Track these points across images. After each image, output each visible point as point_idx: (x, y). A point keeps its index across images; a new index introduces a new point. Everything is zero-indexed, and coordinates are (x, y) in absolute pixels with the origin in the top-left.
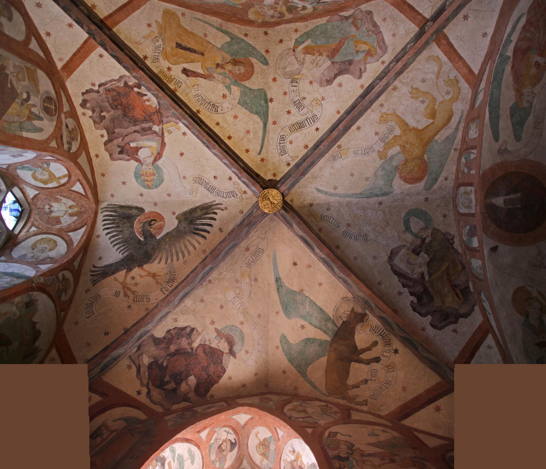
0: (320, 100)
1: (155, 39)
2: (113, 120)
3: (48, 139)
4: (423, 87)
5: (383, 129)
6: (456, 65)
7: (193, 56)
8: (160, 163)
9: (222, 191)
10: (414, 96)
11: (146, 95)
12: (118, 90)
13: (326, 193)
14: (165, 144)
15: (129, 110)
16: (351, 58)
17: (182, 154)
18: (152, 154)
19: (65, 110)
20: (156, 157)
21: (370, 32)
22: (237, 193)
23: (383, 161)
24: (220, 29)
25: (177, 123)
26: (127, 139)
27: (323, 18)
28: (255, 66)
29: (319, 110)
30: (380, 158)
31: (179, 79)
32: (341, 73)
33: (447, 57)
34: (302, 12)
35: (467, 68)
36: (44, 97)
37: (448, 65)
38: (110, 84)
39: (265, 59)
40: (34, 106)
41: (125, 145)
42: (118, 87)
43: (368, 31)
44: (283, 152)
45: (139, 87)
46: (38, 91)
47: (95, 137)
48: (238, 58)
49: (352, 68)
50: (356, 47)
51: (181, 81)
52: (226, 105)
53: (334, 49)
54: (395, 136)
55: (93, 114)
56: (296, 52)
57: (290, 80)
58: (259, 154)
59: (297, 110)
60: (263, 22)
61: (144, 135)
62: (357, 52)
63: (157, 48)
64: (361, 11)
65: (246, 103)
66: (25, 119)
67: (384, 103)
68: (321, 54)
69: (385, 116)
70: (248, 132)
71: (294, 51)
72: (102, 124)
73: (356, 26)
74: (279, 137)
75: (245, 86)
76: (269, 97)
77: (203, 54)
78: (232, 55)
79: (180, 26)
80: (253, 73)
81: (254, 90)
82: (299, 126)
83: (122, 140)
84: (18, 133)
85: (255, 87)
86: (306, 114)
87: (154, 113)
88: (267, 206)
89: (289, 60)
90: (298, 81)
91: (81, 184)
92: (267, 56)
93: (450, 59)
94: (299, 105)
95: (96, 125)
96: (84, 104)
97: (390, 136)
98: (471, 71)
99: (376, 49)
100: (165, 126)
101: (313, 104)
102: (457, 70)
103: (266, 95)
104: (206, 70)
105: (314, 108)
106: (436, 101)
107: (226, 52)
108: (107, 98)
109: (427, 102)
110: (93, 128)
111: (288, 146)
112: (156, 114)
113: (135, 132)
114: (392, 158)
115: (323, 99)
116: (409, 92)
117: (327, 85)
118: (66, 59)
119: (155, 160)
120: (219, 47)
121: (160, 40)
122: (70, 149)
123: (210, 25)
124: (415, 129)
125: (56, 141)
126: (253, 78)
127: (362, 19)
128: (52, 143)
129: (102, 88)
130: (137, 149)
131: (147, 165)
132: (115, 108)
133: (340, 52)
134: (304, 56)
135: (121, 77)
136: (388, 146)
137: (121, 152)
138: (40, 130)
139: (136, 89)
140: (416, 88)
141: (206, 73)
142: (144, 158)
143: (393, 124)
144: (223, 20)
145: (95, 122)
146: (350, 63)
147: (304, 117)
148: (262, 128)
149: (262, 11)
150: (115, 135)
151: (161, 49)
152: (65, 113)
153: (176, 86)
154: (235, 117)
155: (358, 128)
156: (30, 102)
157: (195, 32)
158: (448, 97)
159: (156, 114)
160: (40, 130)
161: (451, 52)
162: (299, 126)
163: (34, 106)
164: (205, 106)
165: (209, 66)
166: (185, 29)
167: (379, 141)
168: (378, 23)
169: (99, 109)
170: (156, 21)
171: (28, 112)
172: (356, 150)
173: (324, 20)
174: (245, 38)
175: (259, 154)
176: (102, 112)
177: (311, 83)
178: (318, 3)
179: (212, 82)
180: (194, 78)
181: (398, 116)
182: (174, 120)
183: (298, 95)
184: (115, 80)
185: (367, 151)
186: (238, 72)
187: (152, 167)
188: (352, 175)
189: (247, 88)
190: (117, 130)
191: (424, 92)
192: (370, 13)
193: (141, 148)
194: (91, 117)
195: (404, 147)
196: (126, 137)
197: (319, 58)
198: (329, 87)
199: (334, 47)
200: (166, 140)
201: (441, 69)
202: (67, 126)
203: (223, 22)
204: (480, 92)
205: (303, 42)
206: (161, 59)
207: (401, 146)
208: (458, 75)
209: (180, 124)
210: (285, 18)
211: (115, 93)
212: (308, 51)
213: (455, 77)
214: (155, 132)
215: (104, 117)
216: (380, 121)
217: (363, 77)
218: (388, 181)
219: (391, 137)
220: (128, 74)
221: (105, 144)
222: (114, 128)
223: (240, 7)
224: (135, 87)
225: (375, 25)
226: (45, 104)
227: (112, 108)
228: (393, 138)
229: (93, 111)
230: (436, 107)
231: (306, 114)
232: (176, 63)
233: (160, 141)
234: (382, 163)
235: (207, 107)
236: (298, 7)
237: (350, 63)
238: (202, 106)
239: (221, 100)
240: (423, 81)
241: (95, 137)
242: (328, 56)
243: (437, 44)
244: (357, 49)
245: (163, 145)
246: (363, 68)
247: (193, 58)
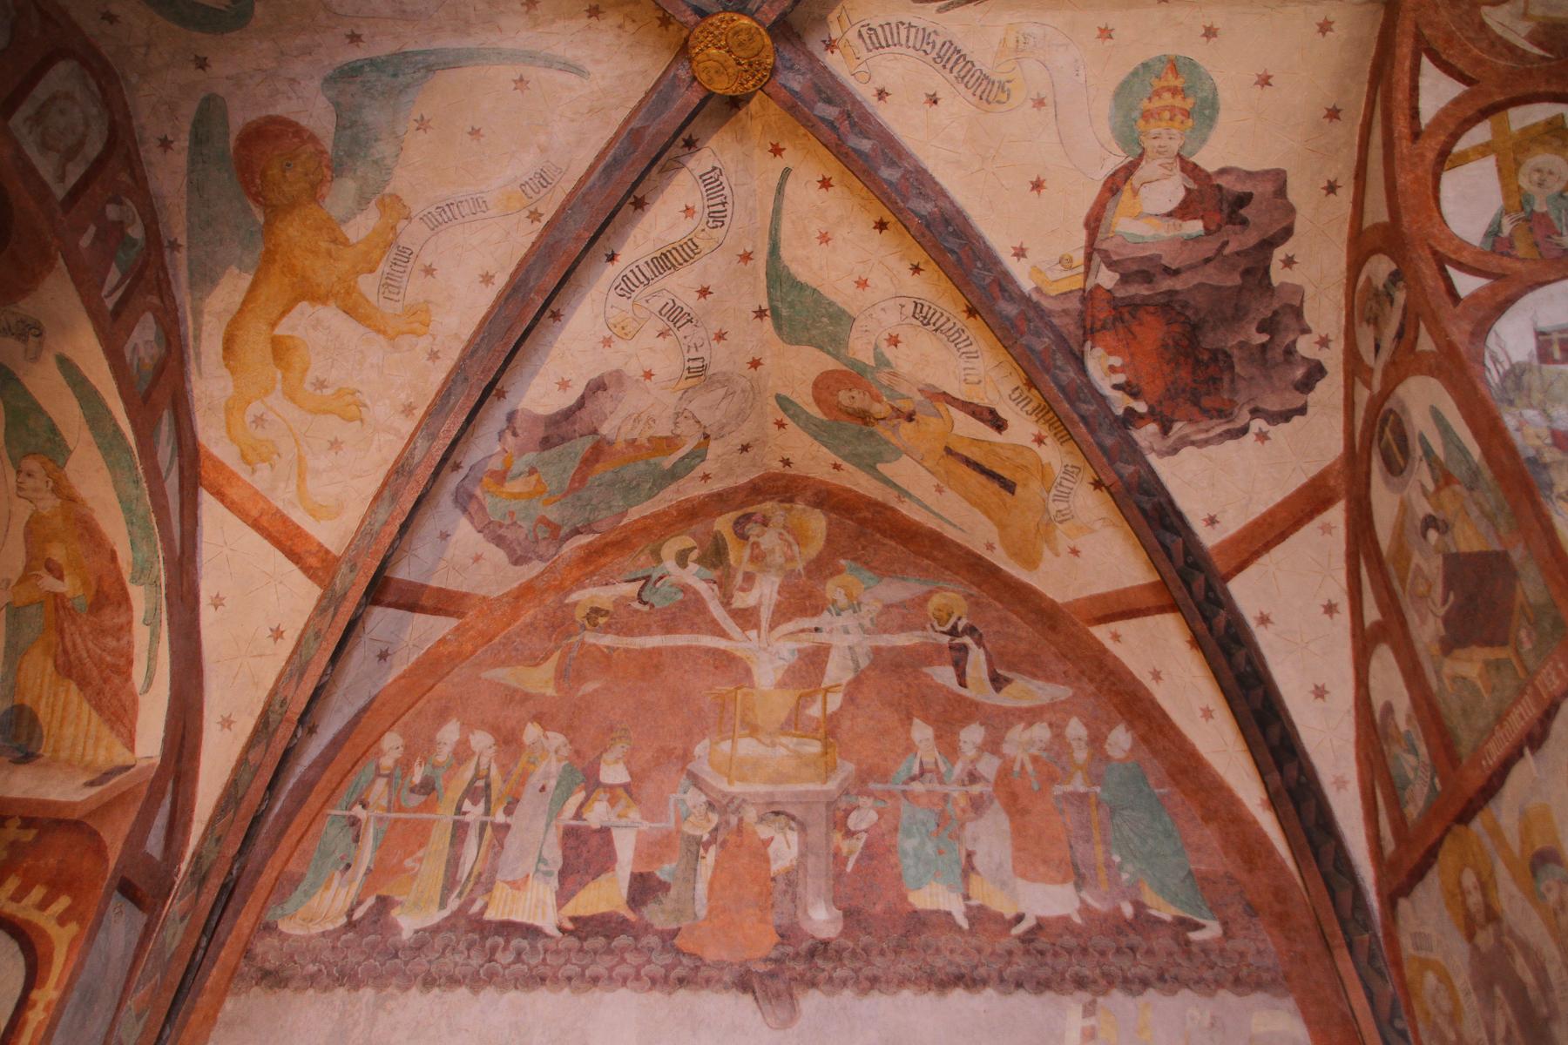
0: (614, 338)
1: (1065, 517)
2: (1238, 316)
4: (332, 426)
5: (414, 288)
6: (261, 504)
7: (976, 454)
8: (1117, 160)
9: (911, 52)
10: (349, 398)
11: (1116, 387)
12: (1195, 410)
13: (549, 63)
14: (1087, 225)
15: (1176, 344)
16: (546, 454)
17: (1037, 186)
18: (1135, 193)
20: (1127, 179)
21: (507, 522)
22: (857, 42)
23: (388, 190)
24: (903, 493)
25: (1038, 290)
26: (1209, 248)
27: (637, 517)
28: (811, 400)
29: (615, 312)
30: (398, 199)
31: (1018, 409)
32: (568, 414)
33: (294, 524)
34: (688, 542)
35: (233, 503)
37: (284, 499)
38: (1212, 434)
39: (785, 410)
41: (1220, 227)
42: (1191, 421)
43: (514, 523)
44: (712, 181)
45: (1130, 411)
47: (1314, 267)
48: (855, 426)
49: (540, 432)
50: (539, 481)
51: (1012, 404)
52: (891, 320)
53: (597, 461)
54: (371, 271)
55: (1294, 342)
56: (700, 435)
57: (709, 372)
58: (787, 172)
59: (678, 303)
60: (791, 500)
61: (1150, 259)
62: (533, 471)
63: (1064, 497)
64: (541, 558)
65: (830, 317)
67: (430, 363)
68: (632, 442)
69: (416, 325)
70: (824, 238)
71: (707, 437)
72: (1276, 305)
73: (548, 523)
74: (727, 220)
75: (837, 357)
76: (768, 321)
77: (949, 451)
78: (872, 434)
79: (1002, 527)
80: (816, 385)
81: (810, 343)
82: (665, 261)
83: (1226, 243)
85: (808, 351)
86: (654, 295)
87: (1103, 327)
88: (743, 37)
89: (718, 414)
90: (686, 374)
91: (1415, 113)
92: (781, 415)
93: (285, 520)
94: (676, 316)
95: (1296, 303)
97: (387, 269)
98: (220, 495)
99: (484, 492)
100: (1077, 284)
101: (635, 324)
102: (256, 493)
103: (778, 328)
104: (944, 413)
105: (631, 314)
106: (284, 393)
107: (887, 443)
108: (1234, 391)
109: (308, 387)
110: (1309, 291)
111: (697, 199)
112: (1098, 325)
113: (1176, 272)
114: (363, 201)
115: (607, 342)
116: (365, 406)
117: (601, 377)
119: (1129, 170)
120: (905, 457)
121: (1053, 513)
123: (926, 507)
124: (316, 296)
126: (814, 372)
127: (537, 541)
129: (1238, 424)
130: (1184, 211)
131: (1160, 152)
132: (1221, 358)
133: (578, 461)
134: (678, 432)
135: (1174, 451)
136: (386, 240)
137: (1244, 200)
139: (1141, 407)
140: (351, 420)
141: (942, 407)
142: (1167, 177)
143: (389, 308)
144: (893, 510)
145: (1298, 313)
146: (546, 443)
147: (656, 286)
148: (783, 245)
149: (790, 545)
150: (1243, 264)
151: (1053, 492)
153: (1026, 393)
154: (862, 284)
155: (487, 279)
157: (966, 504)
158: (255, 408)
159: (1098, 325)
161: (287, 540)
162: (665, 261)
164: (950, 324)
165: (934, 420)
166: (990, 517)
167: (415, 249)
168: (493, 546)
169: (1269, 355)
170: (1057, 555)
172: (480, 215)
173: (635, 514)
174: (839, 461)
175: (787, 172)
176: (1263, 346)
177: (648, 375)
178: (647, 578)
179: (929, 381)
180: (976, 401)
181: (379, 331)
182: (1045, 303)
183: (683, 341)
184: (1193, 443)
185: (444, 215)
186: (855, 393)
187: (1149, 144)
188: (475, 133)
189: (829, 353)
190: (1235, 280)
191: (326, 412)
192: (517, 561)
193: (1170, 215)
195: (334, 241)
196: (1210, 254)
197: (635, 434)
198: (595, 375)
199: (598, 466)
200: (1081, 237)
201: (298, 487)
203: (893, 503)
204: (171, 463)
205: (683, 458)
206: (1057, 469)
207: (346, 243)
208: (249, 480)
209: (1027, 285)
210: (733, 515)
211: (1206, 402)
212: (670, 443)
213: (254, 471)
214: (1111, 265)
215: (1260, 330)
216: (427, 311)
217: (504, 418)
218: (354, 124)
219: (384, 267)
220: (1152, 459)
221: (1288, 232)
222: (1240, 290)
223: (843, 562)
224: (1141, 417)
225: (499, 541)
227: (1228, 356)
228: (378, 263)
229: (1290, 351)
230: (279, 376)
231: (654, 295)
232: (1018, 449)
233: (1100, 236)
234: (387, 182)
235: (943, 320)
236: (699, 561)
237: (546, 443)
238: (959, 325)
239: (904, 333)
240: (335, 445)
241: (1314, 267)
242: (611, 444)
243: (327, 552)
244: (534, 478)
245: (1094, 223)
246: (509, 438)
247: (974, 449)
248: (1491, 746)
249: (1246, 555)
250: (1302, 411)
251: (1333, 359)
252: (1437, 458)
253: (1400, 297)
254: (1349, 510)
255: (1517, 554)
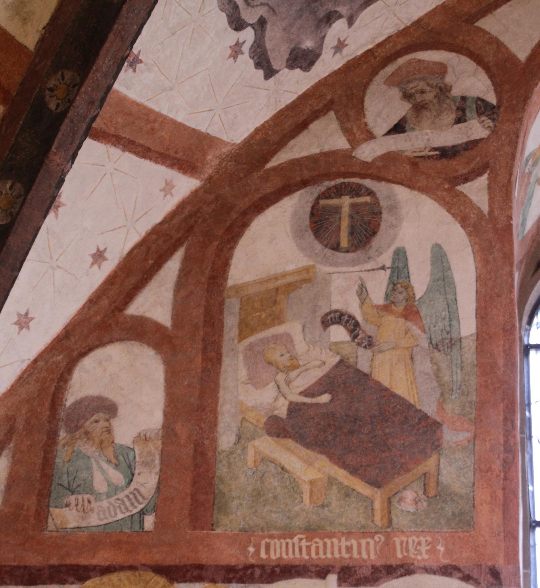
3: (464, 221)
19: (341, 143)
36: (318, 246)
40: (362, 292)
46: (306, 278)
66: (416, 331)
84: (470, 354)
96: (302, 59)
118: (161, 172)
122: (483, 108)
125: (466, 179)
128: (474, 198)
138: (439, 257)
152: (354, 143)
156: (354, 308)
160: (439, 257)
163: (362, 292)
171: (391, 318)
194: (351, 21)
202: (398, 128)
226: (344, 243)
248: (275, 543)
249: (112, 131)
250: (270, 73)
251: (328, 64)
252: (408, 287)
253: (477, 129)
254: (195, 193)
255: (452, 436)
